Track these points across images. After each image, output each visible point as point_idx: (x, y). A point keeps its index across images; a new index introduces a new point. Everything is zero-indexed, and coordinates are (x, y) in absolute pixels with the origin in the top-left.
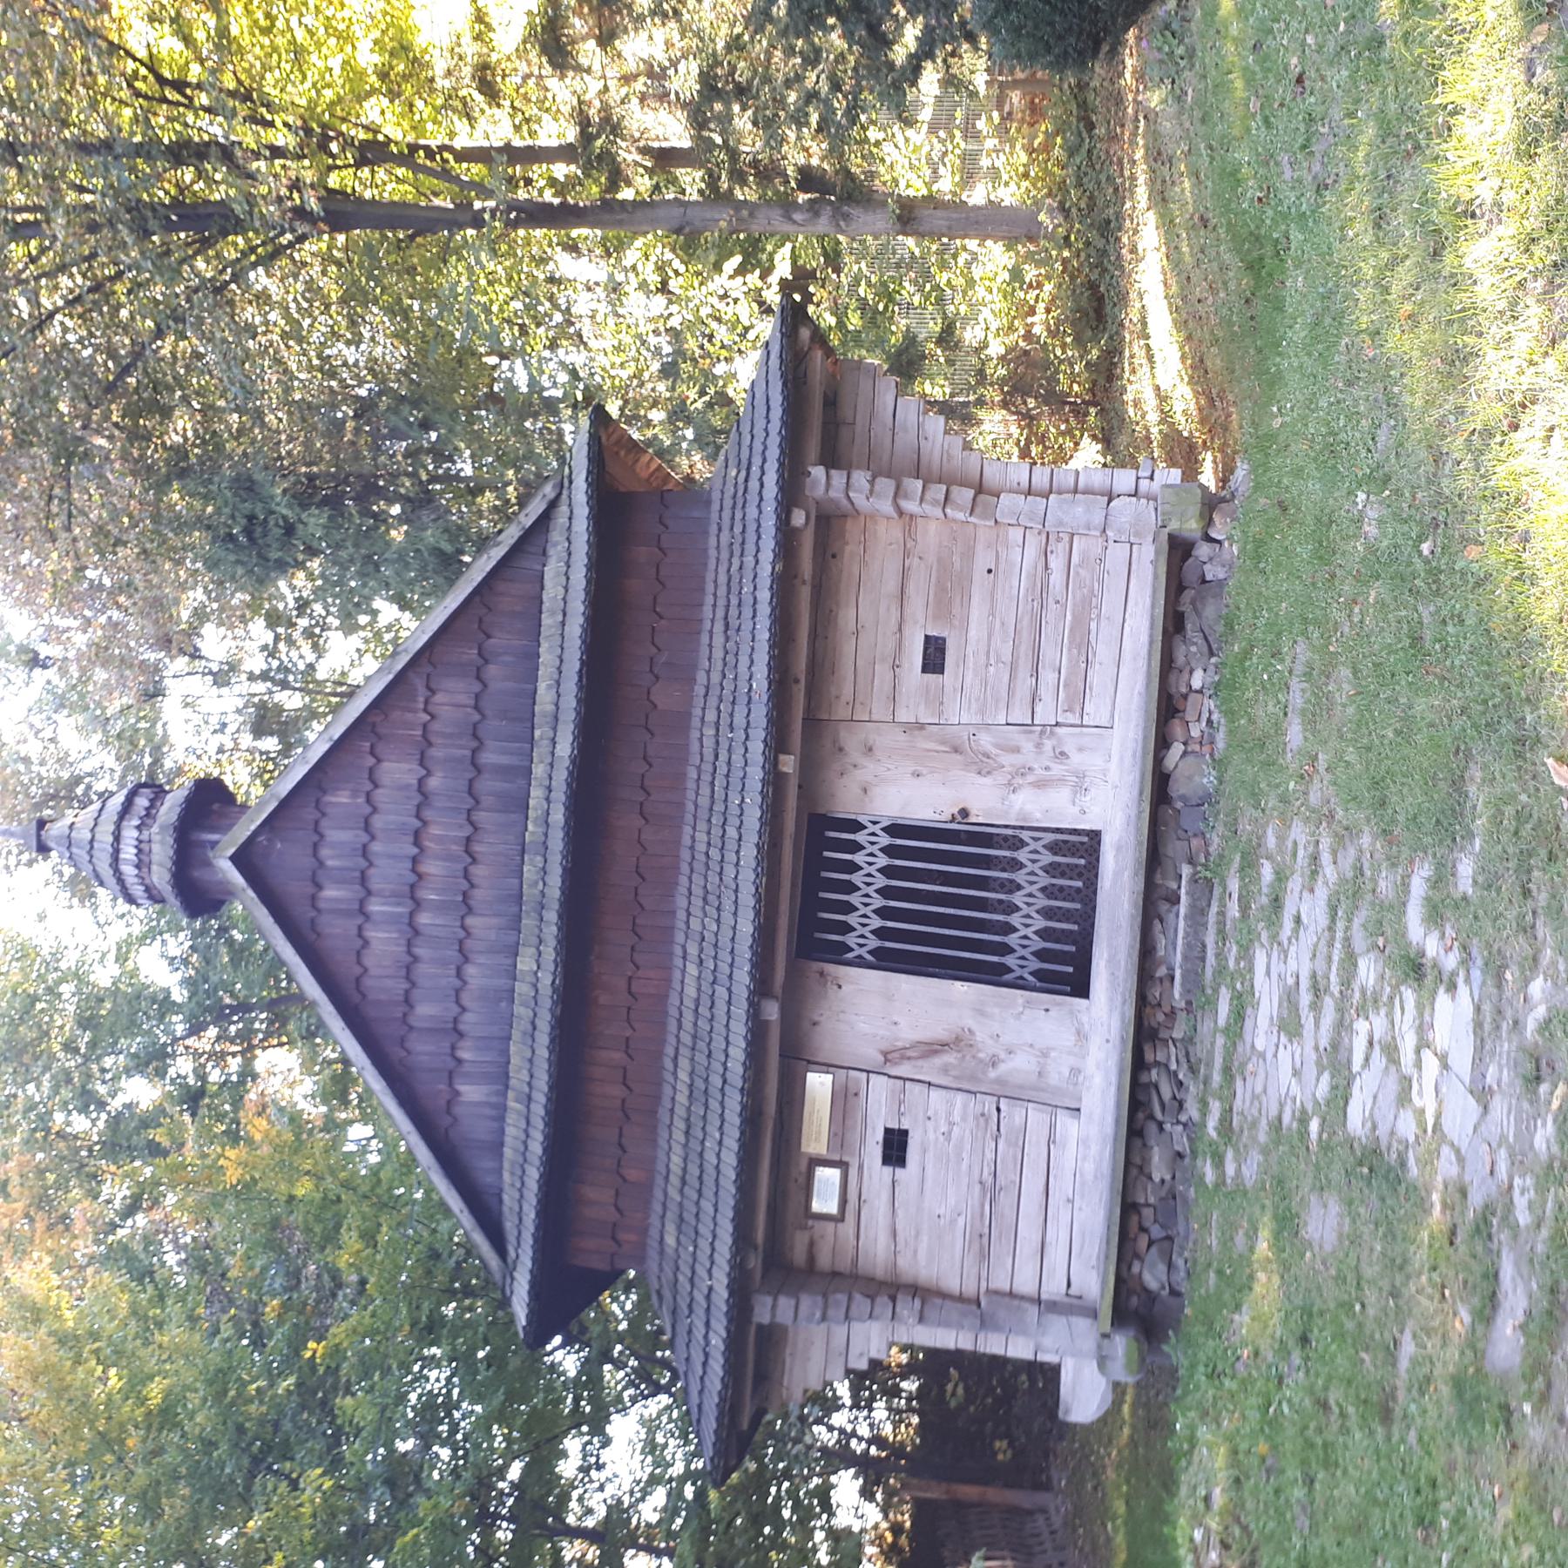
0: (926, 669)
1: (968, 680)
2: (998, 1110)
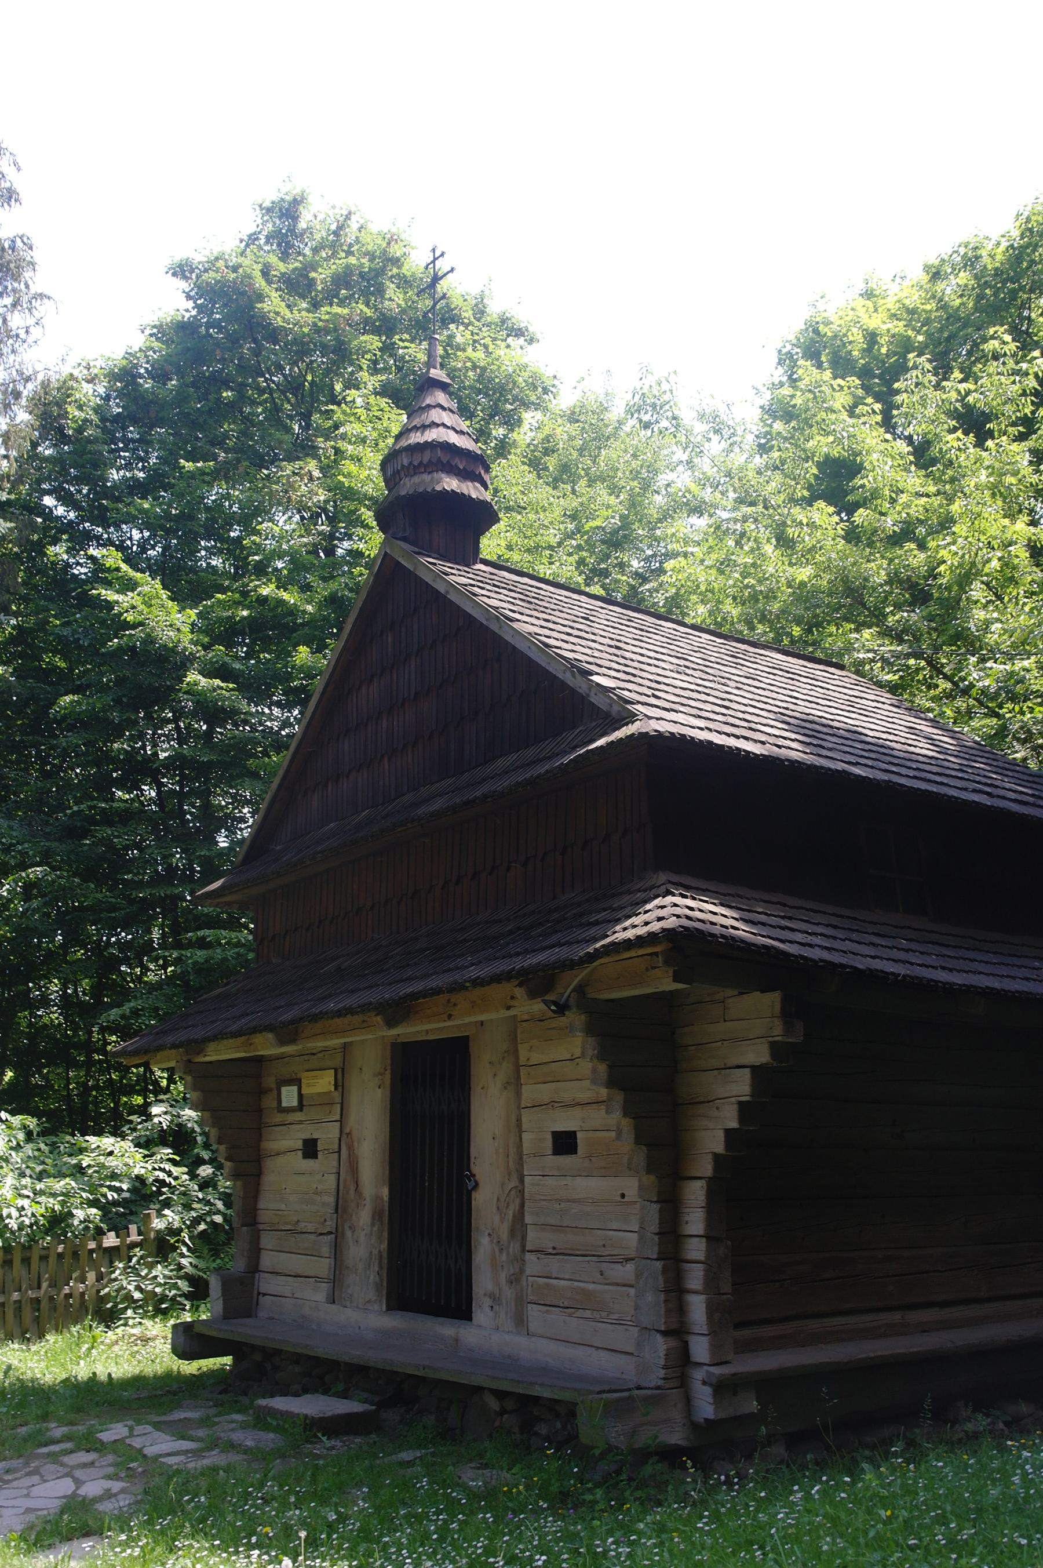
0: (557, 1136)
1: (550, 1181)
2: (330, 1233)
